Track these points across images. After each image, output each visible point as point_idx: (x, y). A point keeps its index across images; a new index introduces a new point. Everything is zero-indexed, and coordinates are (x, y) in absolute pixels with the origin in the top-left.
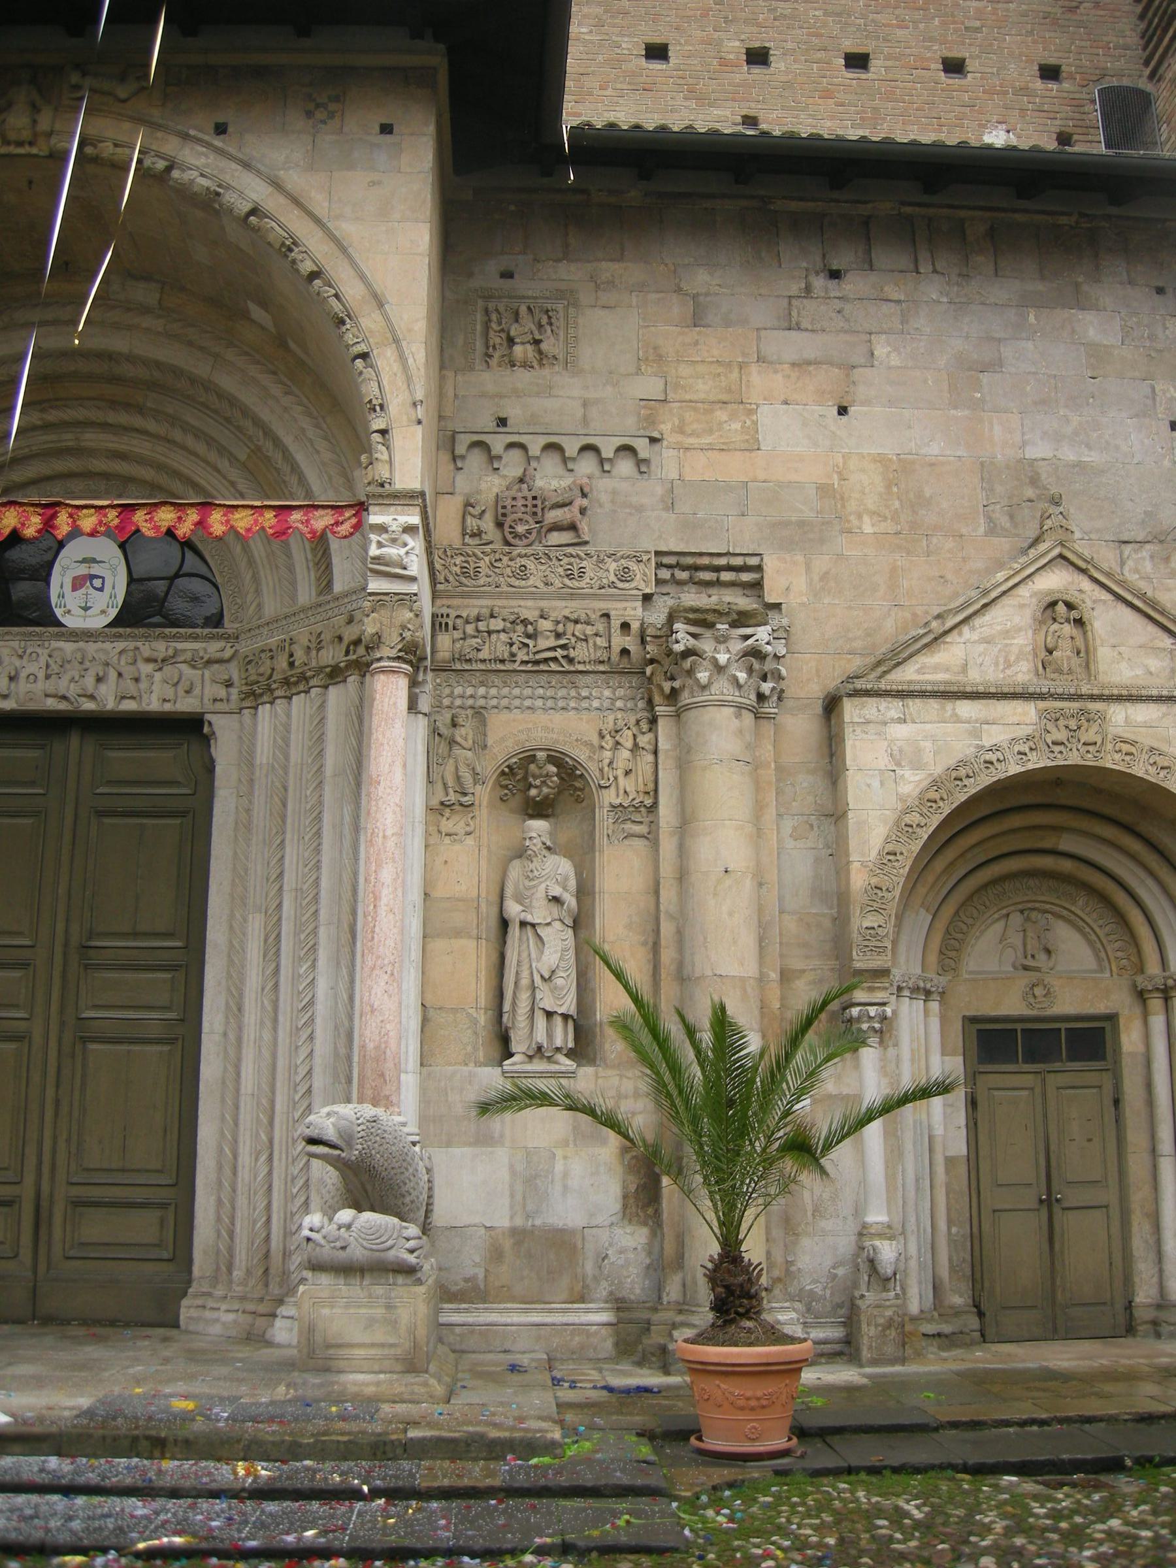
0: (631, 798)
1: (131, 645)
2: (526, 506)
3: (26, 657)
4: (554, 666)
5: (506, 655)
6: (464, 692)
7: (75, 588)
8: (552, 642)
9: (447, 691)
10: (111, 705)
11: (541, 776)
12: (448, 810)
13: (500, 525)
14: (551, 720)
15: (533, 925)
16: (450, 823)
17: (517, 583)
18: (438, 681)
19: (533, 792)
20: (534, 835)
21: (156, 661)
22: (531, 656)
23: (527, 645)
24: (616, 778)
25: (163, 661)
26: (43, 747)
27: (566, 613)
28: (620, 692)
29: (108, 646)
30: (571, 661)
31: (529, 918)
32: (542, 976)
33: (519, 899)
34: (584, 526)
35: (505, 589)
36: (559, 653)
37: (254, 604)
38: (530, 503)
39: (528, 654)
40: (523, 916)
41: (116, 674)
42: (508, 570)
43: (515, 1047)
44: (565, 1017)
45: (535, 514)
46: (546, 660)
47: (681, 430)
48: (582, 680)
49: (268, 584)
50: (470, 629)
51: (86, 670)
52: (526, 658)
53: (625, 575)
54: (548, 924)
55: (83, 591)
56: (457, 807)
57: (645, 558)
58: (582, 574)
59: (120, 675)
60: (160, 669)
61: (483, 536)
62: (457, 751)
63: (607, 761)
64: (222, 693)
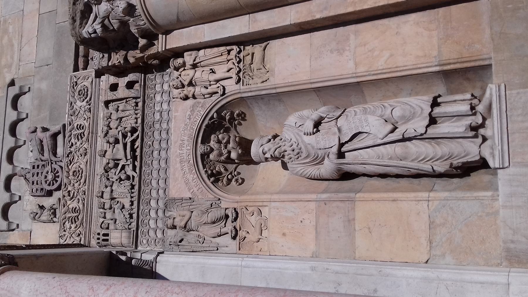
0: (232, 66)
2: (38, 173)
4: (138, 143)
5: (127, 183)
6: (153, 219)
8: (120, 146)
9: (152, 233)
11: (220, 149)
12: (240, 233)
13: (49, 194)
14: (176, 142)
15: (341, 145)
16: (251, 230)
17: (83, 177)
18: (145, 242)
19: (233, 155)
20: (261, 149)
22: (129, 163)
23: (123, 167)
24: (217, 81)
27: (103, 135)
28: (158, 88)
30: (134, 130)
31: (335, 149)
32: (392, 131)
33: (319, 161)
34: (54, 129)
35: (86, 187)
36: (129, 140)
38: (36, 171)
39: (128, 165)
40: (333, 157)
42: (76, 185)
43: (473, 157)
44: (435, 103)
45: (44, 165)
46: (133, 150)
47: (10, 66)
48: (148, 120)
50: (109, 215)
52: (131, 166)
53: (84, 94)
54: (339, 130)
56: (238, 224)
57: (75, 80)
58: (80, 127)
61: (54, 207)
62: (193, 224)
63: (204, 91)
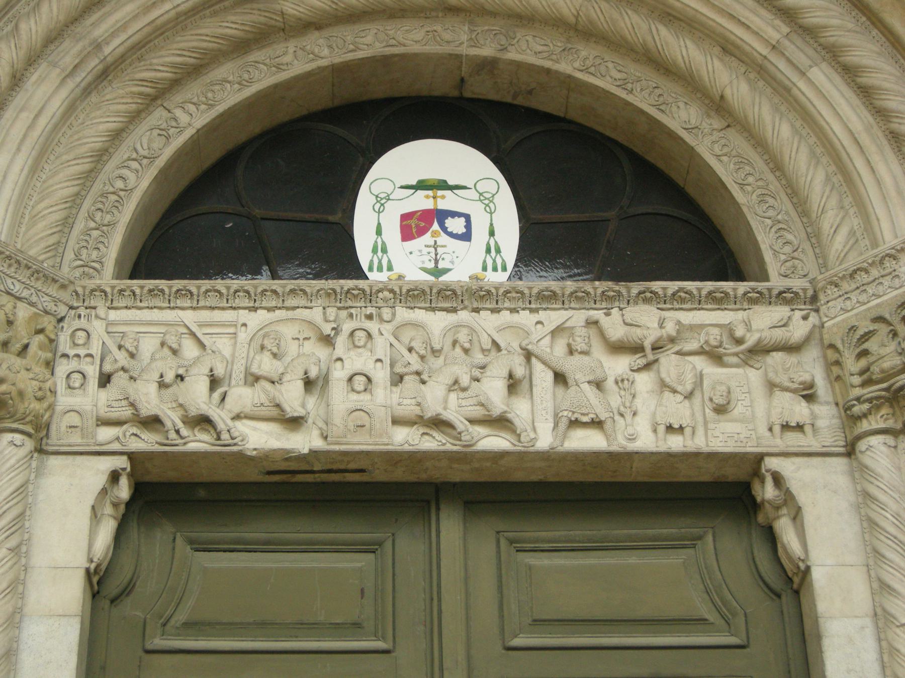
1: (577, 317)
3: (341, 342)
7: (407, 234)
10: (545, 440)
21: (637, 349)
25: (655, 348)
26: (370, 548)
29: (525, 318)
37: (844, 231)
41: (550, 376)
49: (879, 182)
51: (483, 367)
55: (427, 239)
59: (560, 378)
60: (647, 367)
64: (800, 411)
